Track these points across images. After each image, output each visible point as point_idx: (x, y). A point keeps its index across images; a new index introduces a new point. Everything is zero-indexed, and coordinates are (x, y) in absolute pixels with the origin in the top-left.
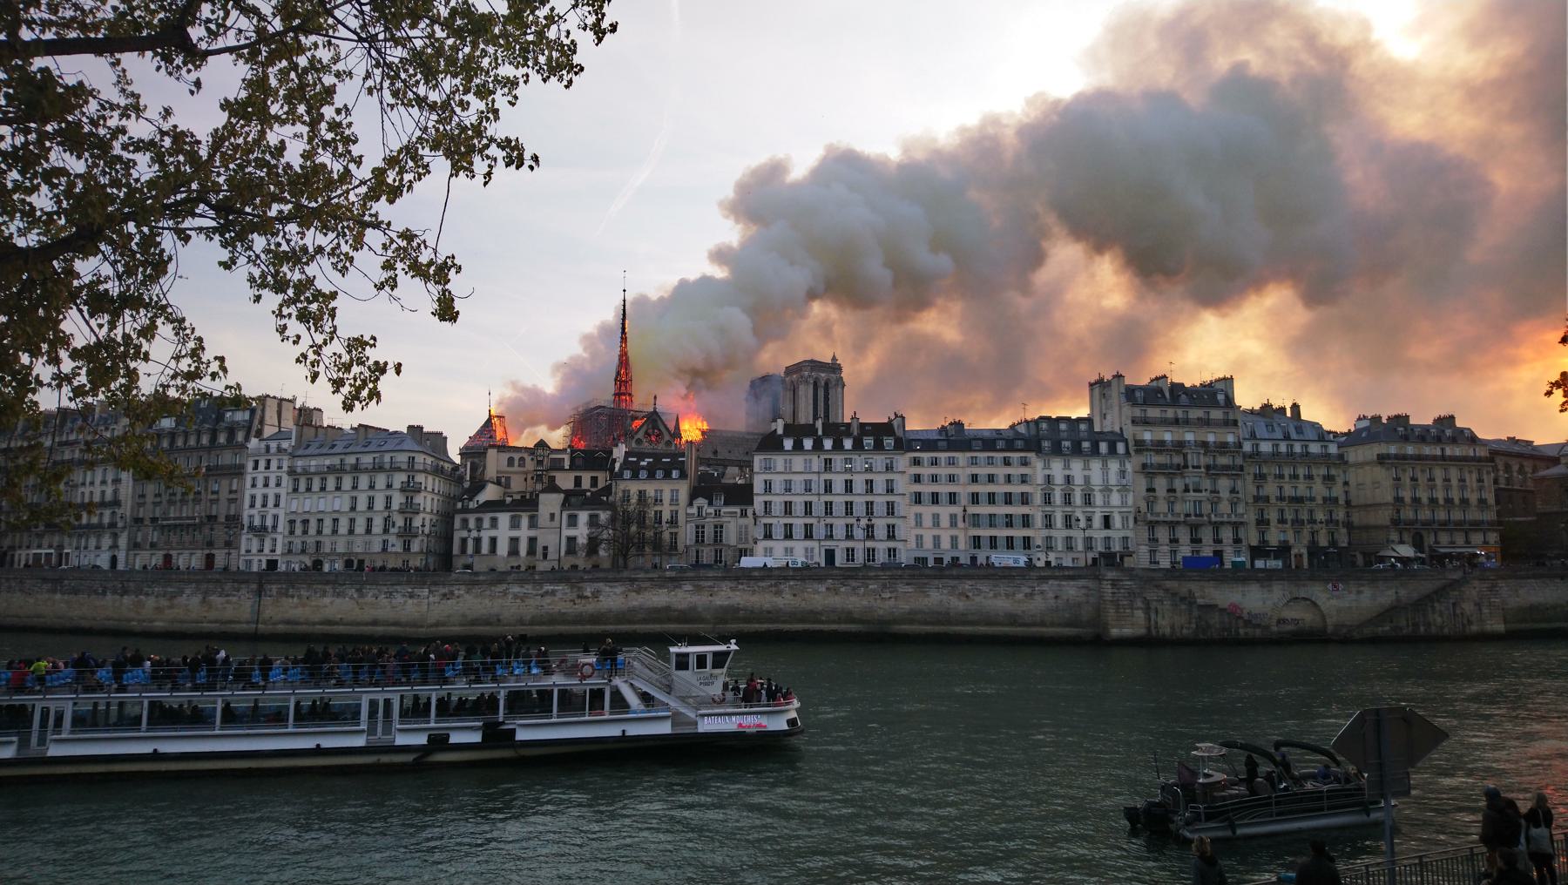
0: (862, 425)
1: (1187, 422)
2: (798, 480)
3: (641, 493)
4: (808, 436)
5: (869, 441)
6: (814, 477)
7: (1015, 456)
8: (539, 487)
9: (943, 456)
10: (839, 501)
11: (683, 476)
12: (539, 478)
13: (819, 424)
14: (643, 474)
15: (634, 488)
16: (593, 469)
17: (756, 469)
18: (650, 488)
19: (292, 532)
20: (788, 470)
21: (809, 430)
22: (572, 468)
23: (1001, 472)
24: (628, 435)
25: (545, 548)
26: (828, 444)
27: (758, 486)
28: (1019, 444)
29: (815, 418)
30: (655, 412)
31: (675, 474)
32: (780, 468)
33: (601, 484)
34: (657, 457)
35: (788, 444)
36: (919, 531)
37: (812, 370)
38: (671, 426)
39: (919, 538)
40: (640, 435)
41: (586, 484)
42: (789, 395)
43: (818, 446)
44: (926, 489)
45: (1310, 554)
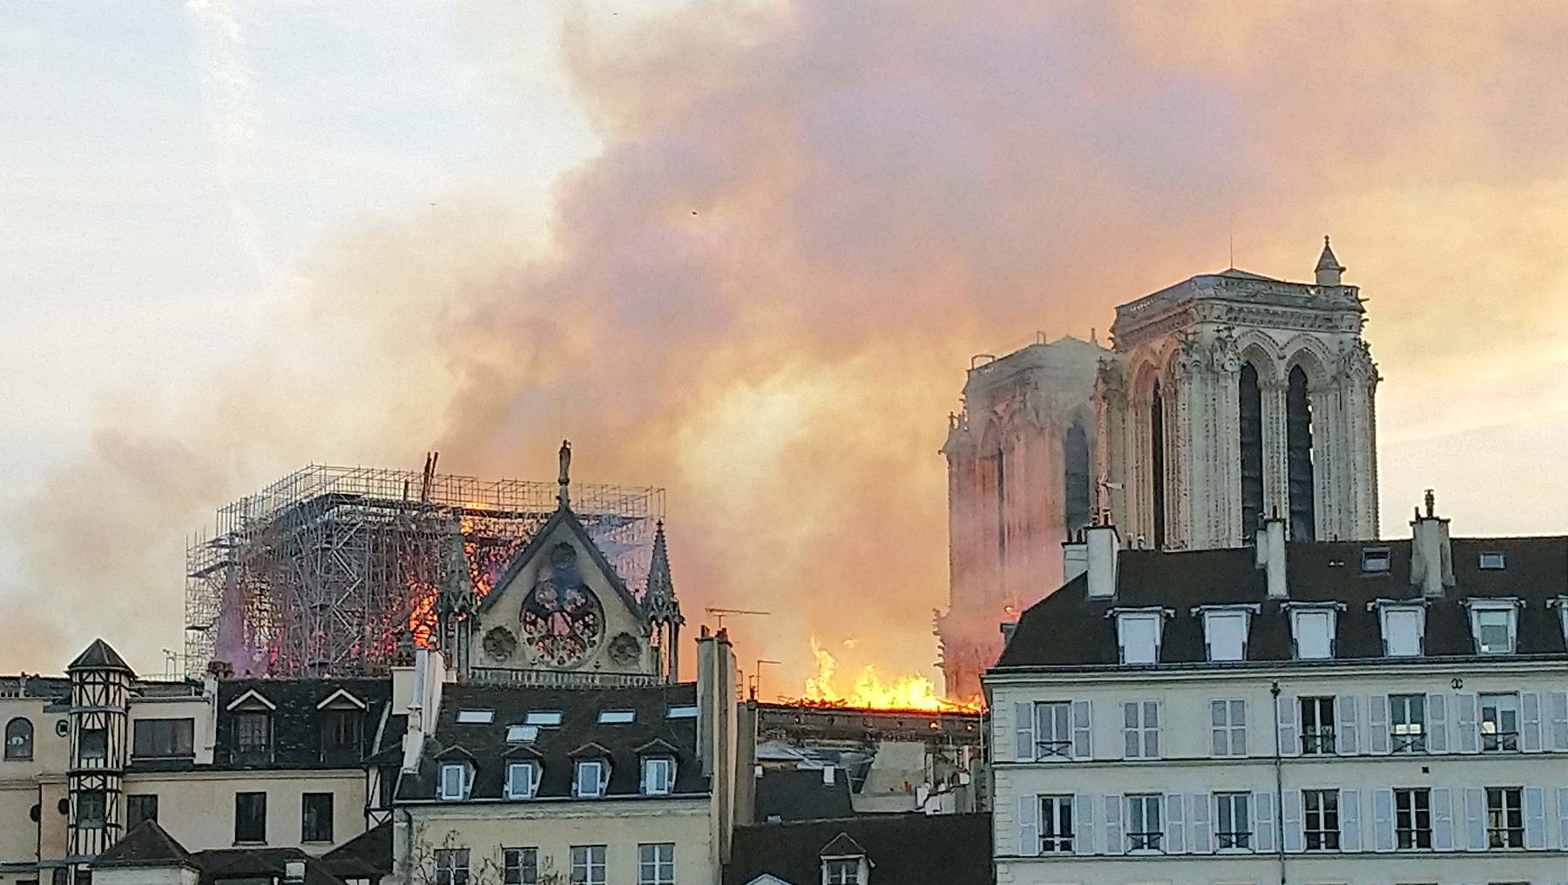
0: (1465, 552)
2: (1189, 798)
3: (516, 863)
4: (1226, 599)
5: (1495, 621)
6: (1259, 781)
8: (91, 843)
11: (691, 781)
12: (90, 805)
13: (1272, 549)
14: (522, 779)
15: (484, 836)
16: (313, 764)
17: (1004, 746)
18: (553, 836)
20: (1143, 751)
21: (1231, 575)
22: (227, 759)
24: (457, 616)
26: (1314, 633)
27: (1015, 827)
29: (1254, 522)
30: (564, 512)
31: (655, 774)
32: (1107, 739)
33: (347, 827)
34: (578, 705)
35: (1140, 636)
37: (1233, 317)
38: (638, 587)
40: (505, 614)
41: (283, 827)
42: (1135, 431)
43: (1270, 645)
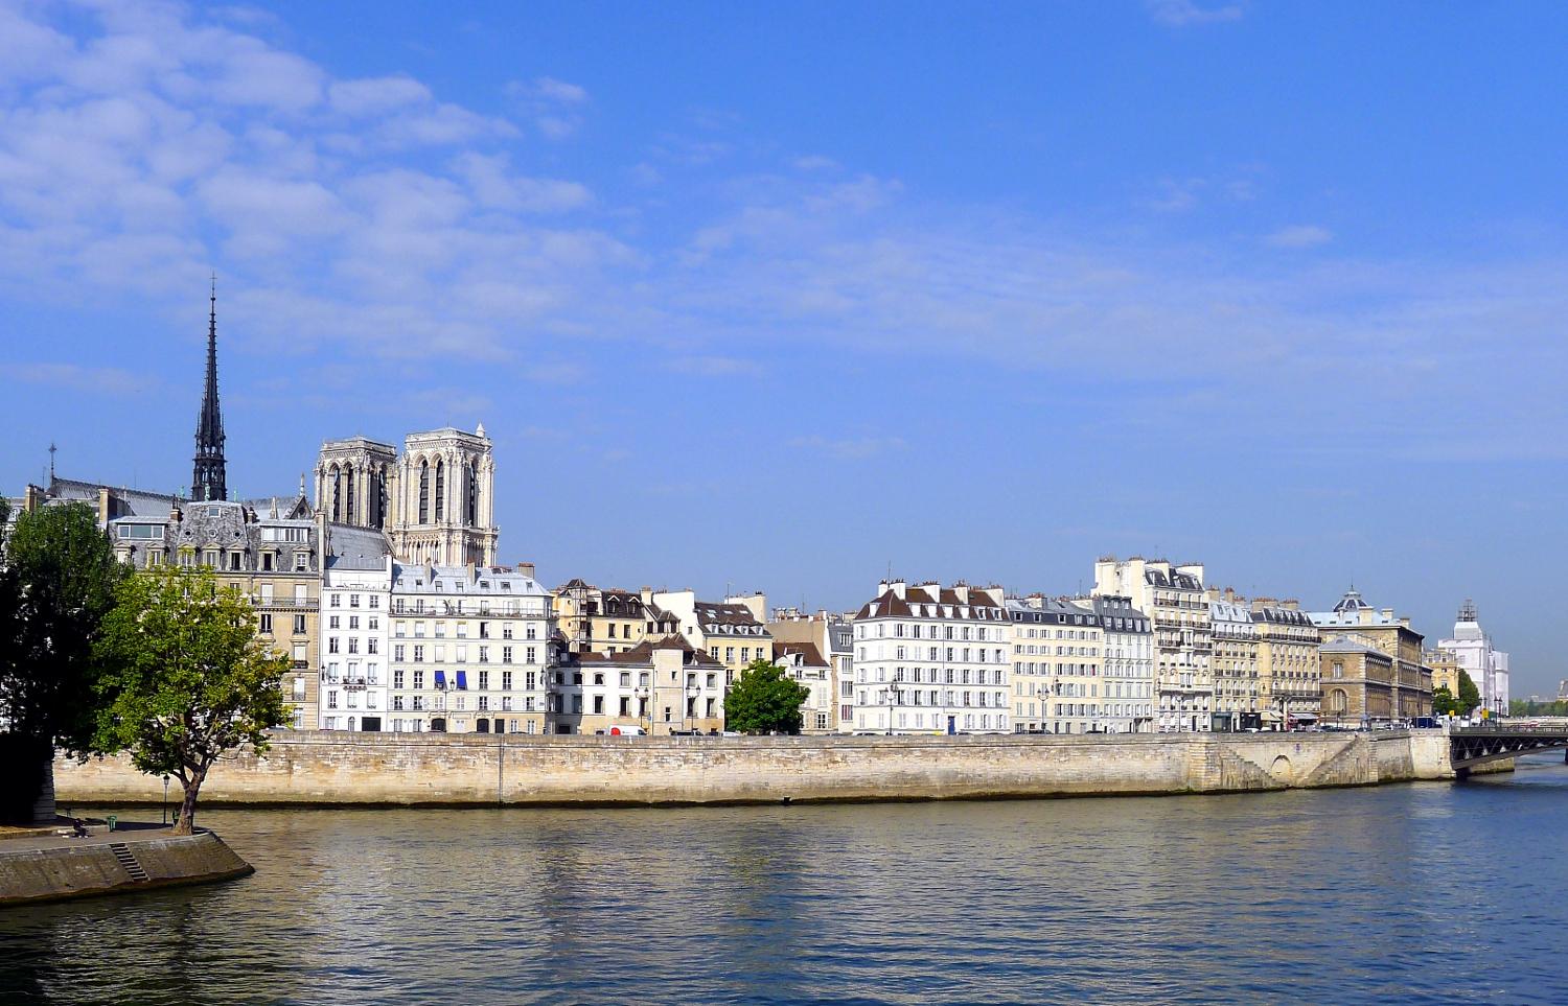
1: (1176, 603)
7: (1089, 630)
9: (1039, 628)
10: (958, 669)
19: (398, 684)
23: (1077, 644)
25: (668, 710)
28: (1091, 621)
36: (1019, 699)
39: (1019, 705)
44: (1025, 659)
45: (1241, 718)
